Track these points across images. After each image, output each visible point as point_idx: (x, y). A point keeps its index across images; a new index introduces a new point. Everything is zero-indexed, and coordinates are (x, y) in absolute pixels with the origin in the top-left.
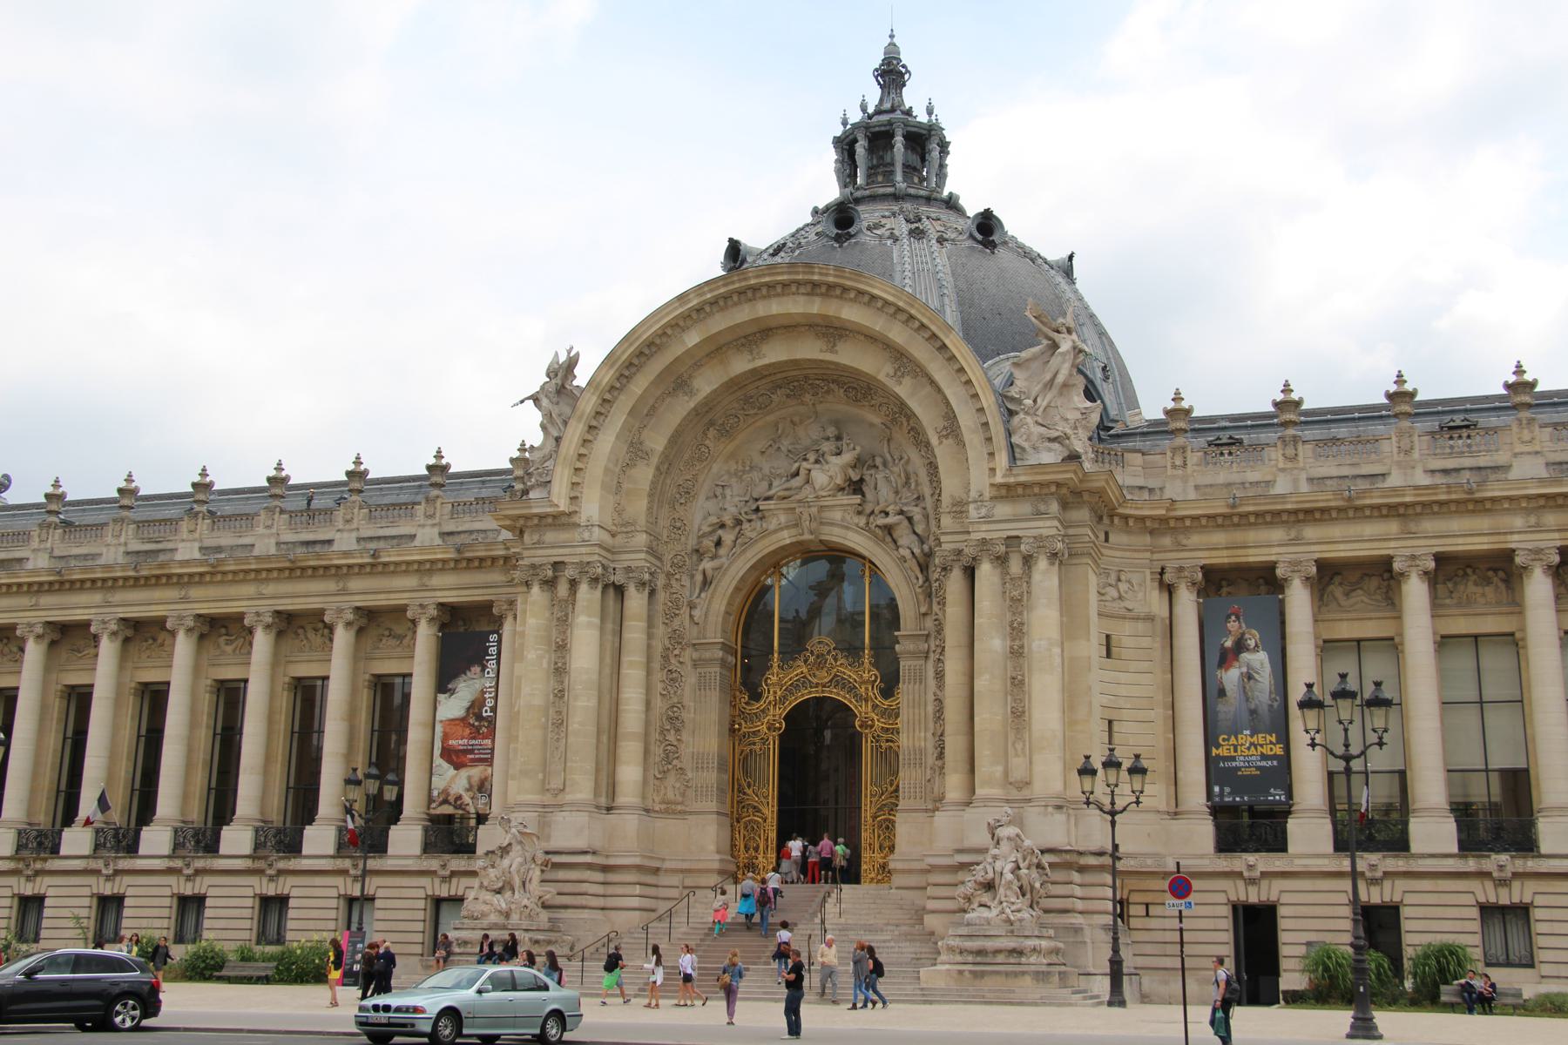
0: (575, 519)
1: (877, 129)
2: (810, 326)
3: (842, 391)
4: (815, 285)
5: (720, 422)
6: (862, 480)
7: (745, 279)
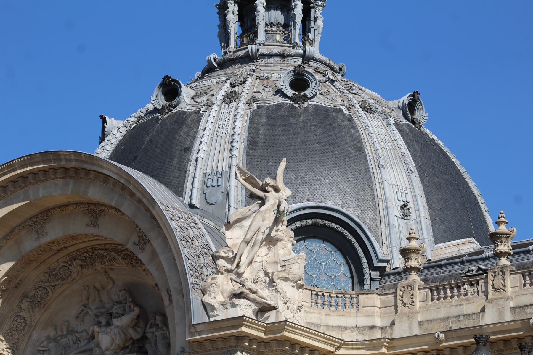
2: (77, 204)
4: (66, 170)
5: (32, 294)
6: (144, 338)
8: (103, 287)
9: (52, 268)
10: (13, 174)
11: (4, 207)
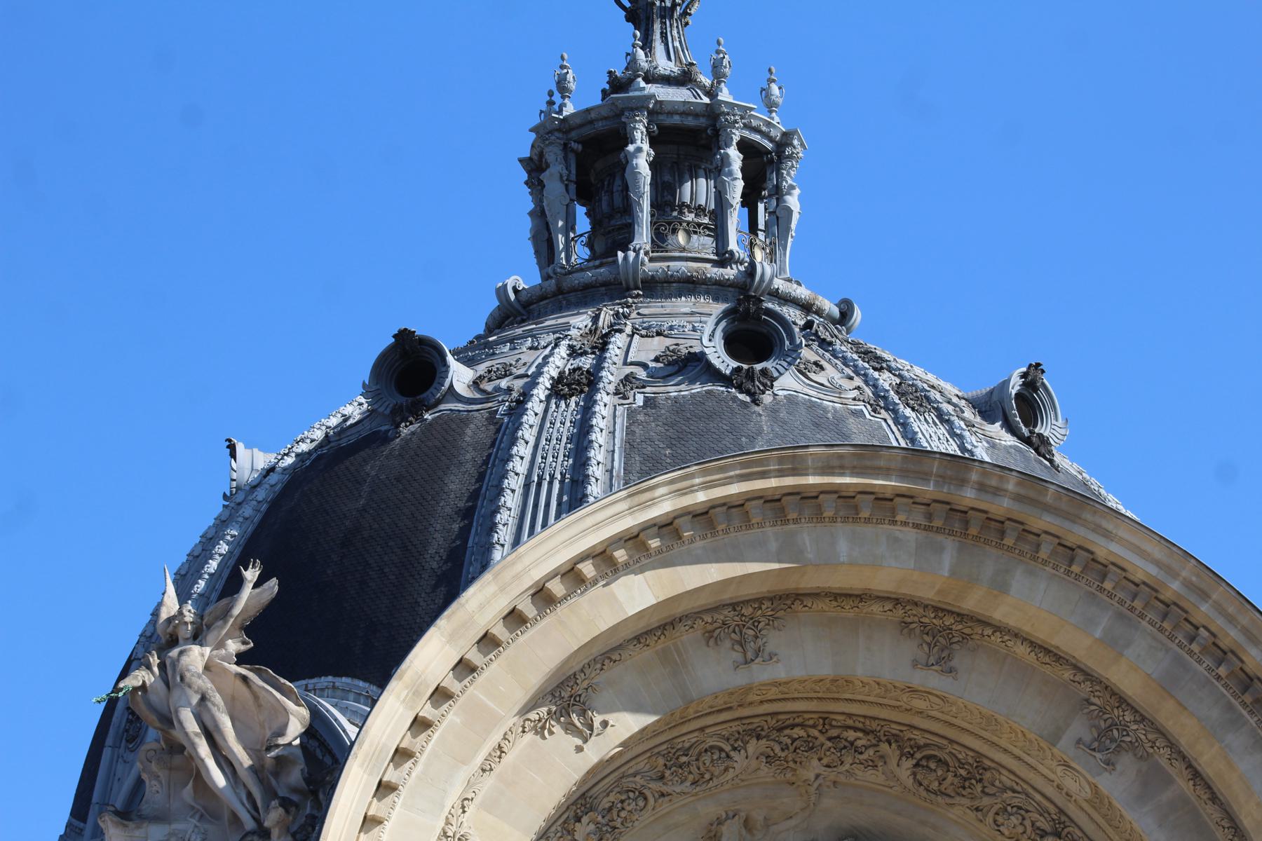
1: (676, 120)
2: (897, 601)
3: (910, 763)
5: (605, 804)
7: (795, 472)
8: (768, 823)
9: (680, 746)
11: (710, 562)
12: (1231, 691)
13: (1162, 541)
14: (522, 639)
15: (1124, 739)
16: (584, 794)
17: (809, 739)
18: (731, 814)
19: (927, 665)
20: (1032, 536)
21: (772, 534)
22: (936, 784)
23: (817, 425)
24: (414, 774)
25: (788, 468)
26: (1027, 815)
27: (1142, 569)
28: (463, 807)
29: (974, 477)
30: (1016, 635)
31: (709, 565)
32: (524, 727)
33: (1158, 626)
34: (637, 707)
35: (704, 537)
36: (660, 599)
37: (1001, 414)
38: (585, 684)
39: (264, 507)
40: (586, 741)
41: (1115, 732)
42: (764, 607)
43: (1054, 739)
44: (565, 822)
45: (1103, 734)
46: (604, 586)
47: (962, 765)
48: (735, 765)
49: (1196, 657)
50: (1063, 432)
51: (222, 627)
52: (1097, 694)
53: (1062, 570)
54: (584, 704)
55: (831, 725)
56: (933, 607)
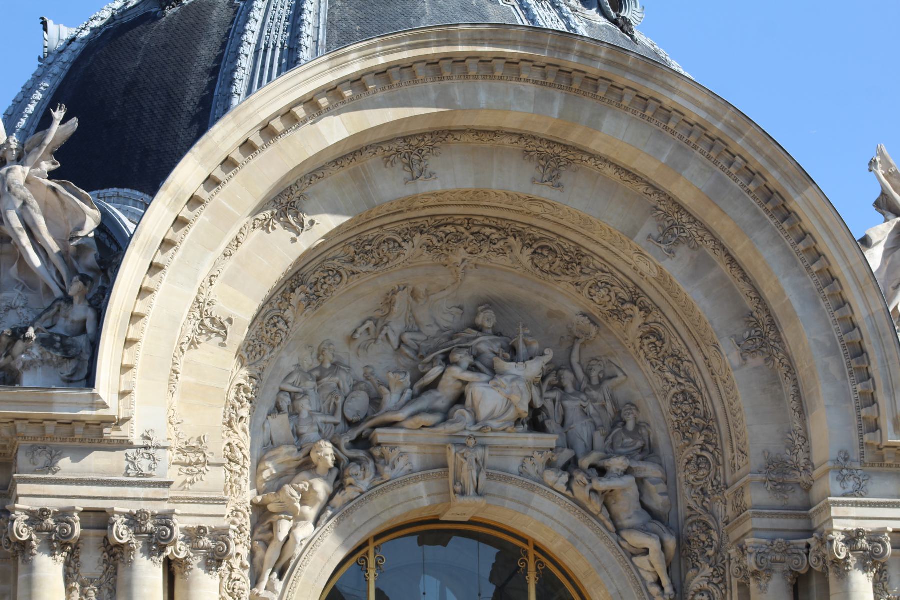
0: (124, 432)
2: (521, 136)
5: (313, 279)
7: (449, 43)
8: (428, 294)
9: (365, 239)
10: (445, 50)
11: (388, 107)
12: (758, 201)
13: (710, 94)
14: (253, 162)
15: (682, 235)
16: (297, 273)
17: (458, 234)
18: (402, 287)
19: (542, 182)
20: (617, 90)
21: (432, 88)
22: (548, 266)
23: (465, 10)
24: (176, 258)
25: (444, 41)
26: (612, 289)
27: (696, 114)
28: (211, 282)
29: (577, 47)
30: (606, 161)
31: (387, 110)
32: (254, 225)
33: (706, 154)
34: (335, 211)
35: (383, 90)
36: (352, 134)
37: (597, 2)
38: (298, 194)
39: (68, 67)
40: (298, 234)
41: (675, 230)
42: (426, 140)
43: (632, 235)
44: (283, 293)
45: (667, 231)
46: (312, 124)
47: (566, 253)
48: (405, 252)
49: (733, 177)
50: (640, 15)
51: (38, 153)
52: (662, 203)
53: (639, 114)
54: (297, 208)
55: (473, 224)
56: (547, 140)
